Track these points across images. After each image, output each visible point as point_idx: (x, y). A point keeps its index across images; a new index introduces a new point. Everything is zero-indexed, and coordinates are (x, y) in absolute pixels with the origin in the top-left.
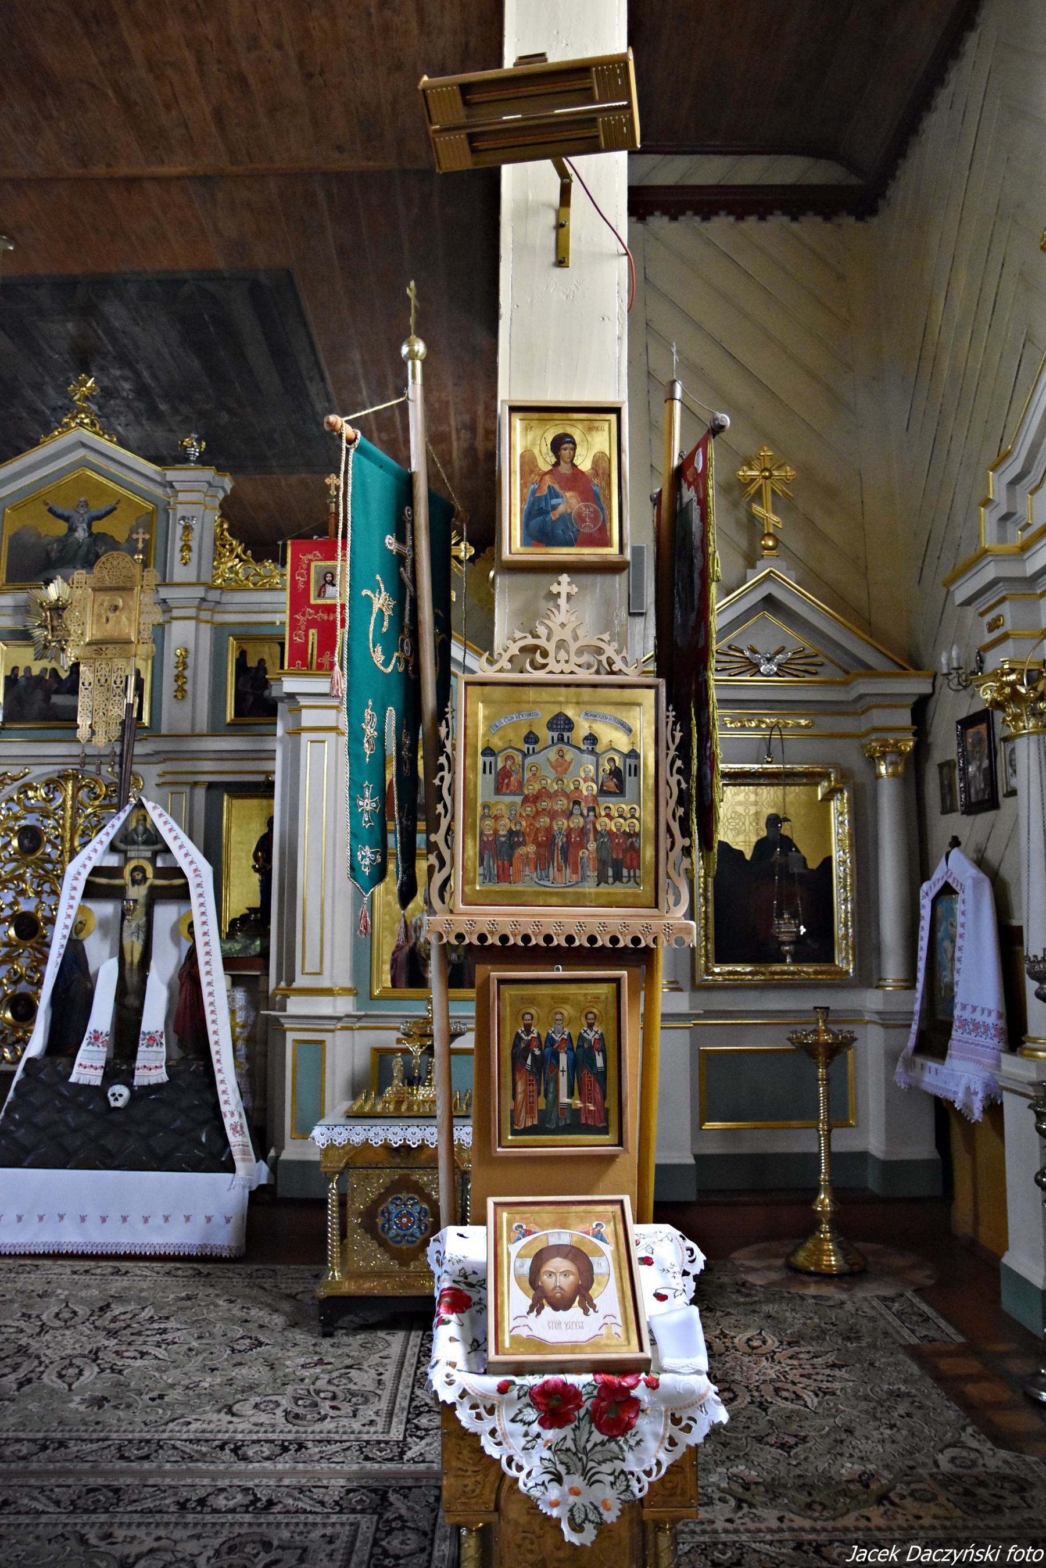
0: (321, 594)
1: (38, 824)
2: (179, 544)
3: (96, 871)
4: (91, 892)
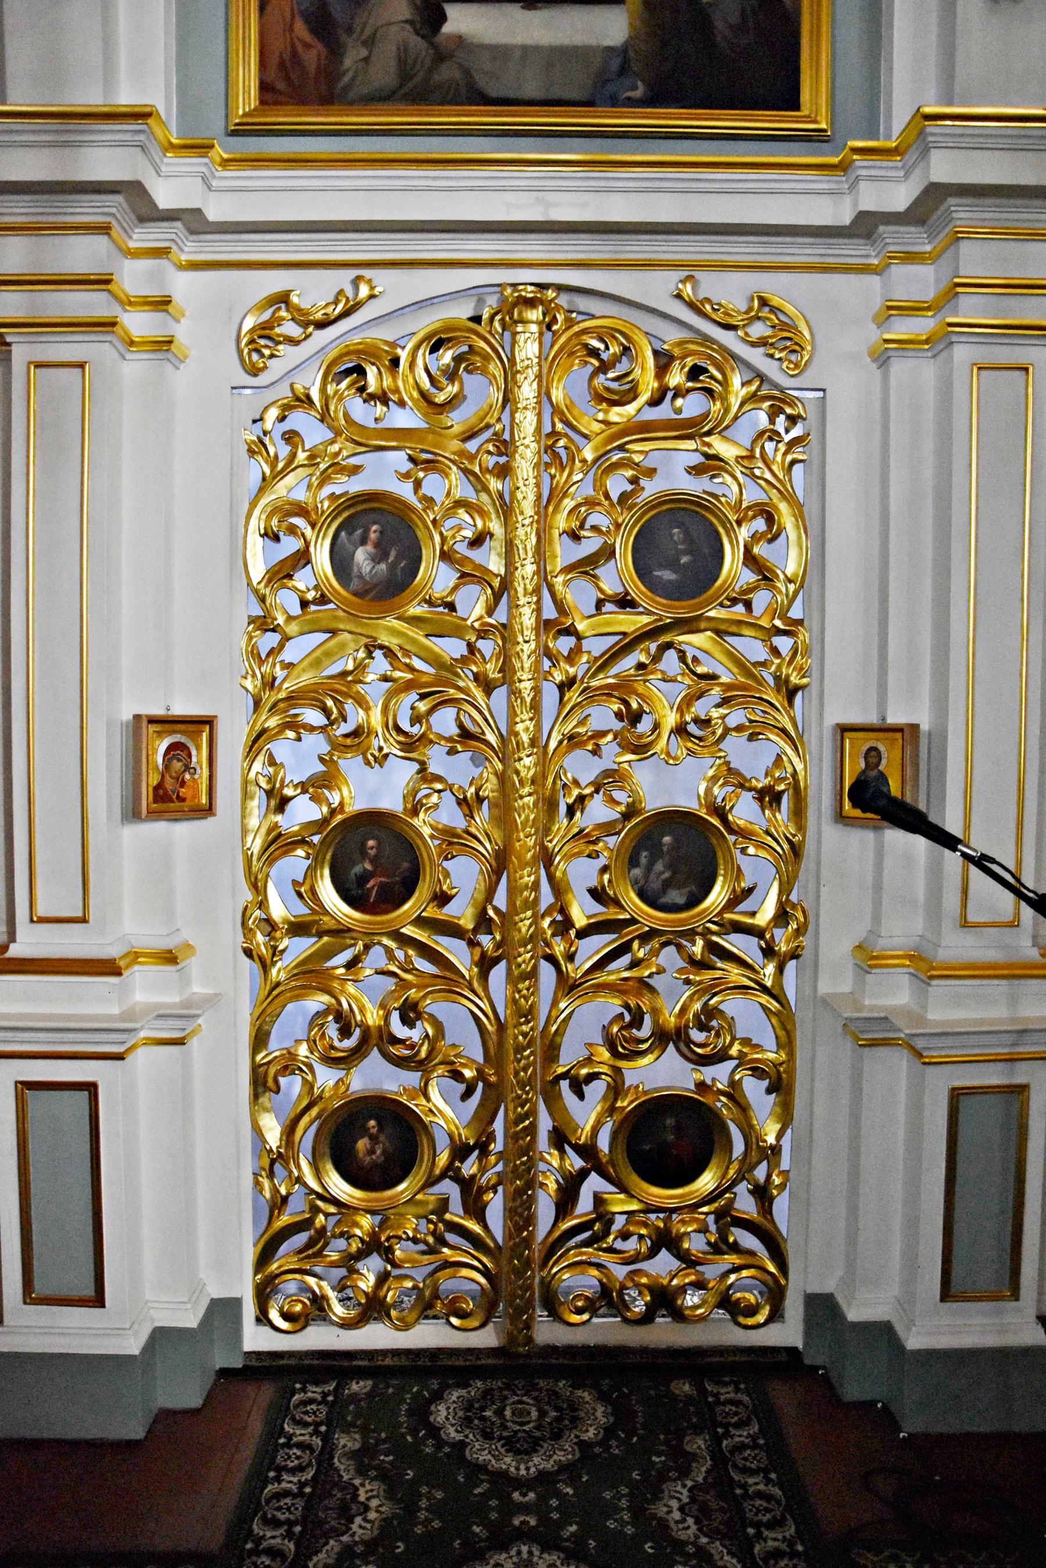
1: (405, 491)
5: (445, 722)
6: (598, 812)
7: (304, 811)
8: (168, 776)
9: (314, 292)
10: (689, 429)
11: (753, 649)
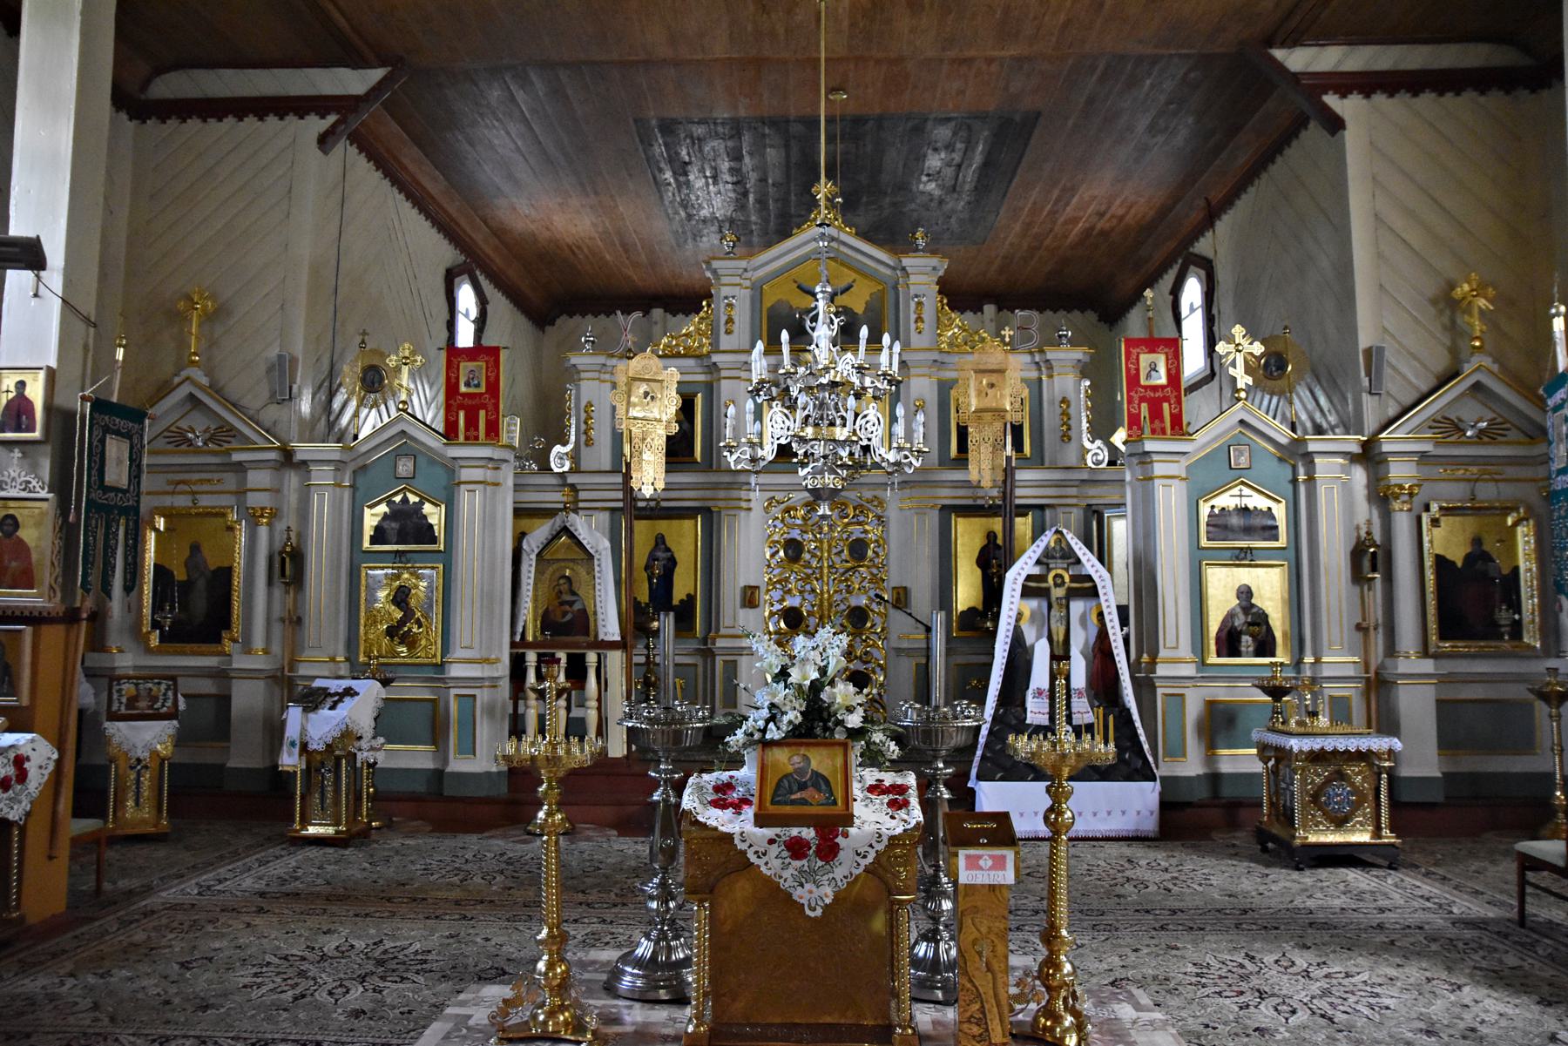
0: (1148, 376)
2: (913, 317)
3: (1029, 578)
4: (1027, 592)
5: (808, 587)
6: (842, 607)
7: (777, 607)
8: (750, 598)
9: (779, 496)
10: (859, 523)
11: (875, 571)
